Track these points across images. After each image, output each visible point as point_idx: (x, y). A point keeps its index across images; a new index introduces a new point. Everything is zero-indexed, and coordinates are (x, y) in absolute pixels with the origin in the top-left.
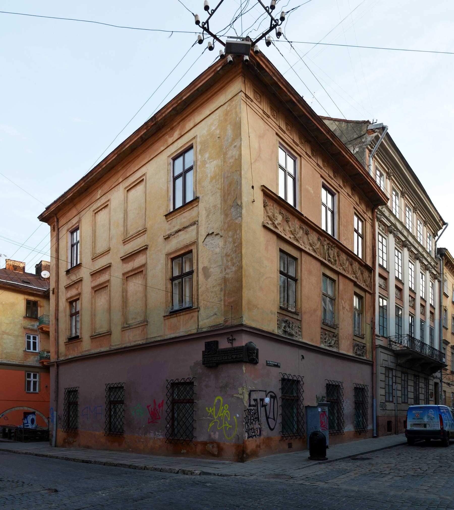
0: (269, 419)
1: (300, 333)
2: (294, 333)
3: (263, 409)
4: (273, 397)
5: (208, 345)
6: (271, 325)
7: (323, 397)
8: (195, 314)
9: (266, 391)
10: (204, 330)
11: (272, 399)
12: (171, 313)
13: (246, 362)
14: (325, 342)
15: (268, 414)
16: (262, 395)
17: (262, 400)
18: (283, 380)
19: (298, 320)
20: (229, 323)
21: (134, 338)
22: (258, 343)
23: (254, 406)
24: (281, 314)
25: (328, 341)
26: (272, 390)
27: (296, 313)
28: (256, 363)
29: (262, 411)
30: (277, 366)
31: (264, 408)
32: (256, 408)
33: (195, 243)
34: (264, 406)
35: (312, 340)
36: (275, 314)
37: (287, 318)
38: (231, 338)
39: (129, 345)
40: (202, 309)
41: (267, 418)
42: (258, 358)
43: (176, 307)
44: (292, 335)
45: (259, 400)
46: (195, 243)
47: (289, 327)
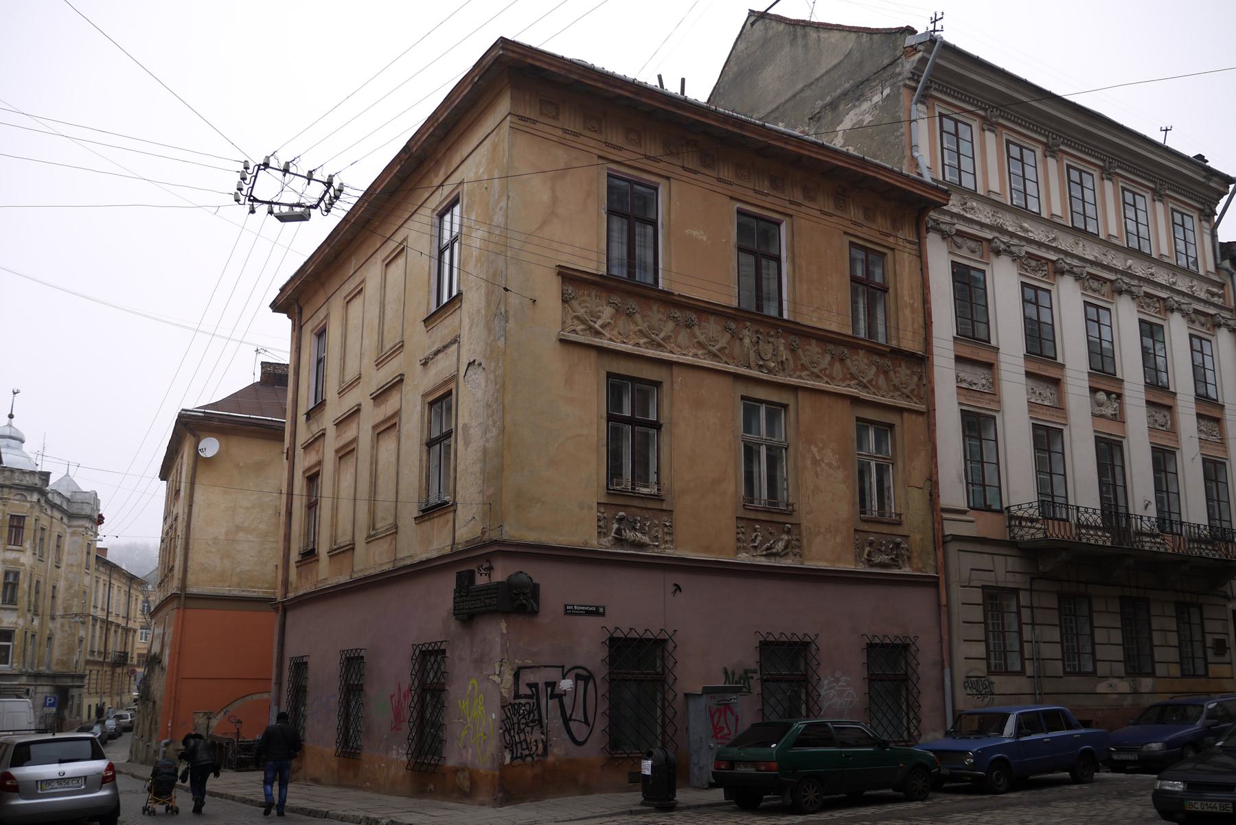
0: (571, 723)
1: (668, 538)
2: (646, 539)
4: (584, 677)
5: (460, 576)
6: (582, 532)
7: (746, 672)
8: (451, 516)
9: (563, 667)
10: (460, 548)
11: (581, 684)
12: (423, 511)
13: (506, 613)
14: (755, 547)
15: (568, 713)
16: (553, 675)
17: (552, 684)
18: (612, 639)
20: (486, 537)
21: (372, 559)
22: (538, 572)
23: (526, 696)
25: (762, 543)
26: (580, 663)
27: (657, 498)
28: (535, 613)
29: (550, 709)
30: (596, 612)
33: (454, 378)
34: (560, 697)
35: (707, 549)
36: (591, 508)
37: (621, 513)
38: (487, 565)
39: (373, 572)
40: (459, 506)
41: (566, 720)
42: (537, 600)
43: (434, 500)
44: (641, 545)
46: (454, 378)
47: (634, 529)
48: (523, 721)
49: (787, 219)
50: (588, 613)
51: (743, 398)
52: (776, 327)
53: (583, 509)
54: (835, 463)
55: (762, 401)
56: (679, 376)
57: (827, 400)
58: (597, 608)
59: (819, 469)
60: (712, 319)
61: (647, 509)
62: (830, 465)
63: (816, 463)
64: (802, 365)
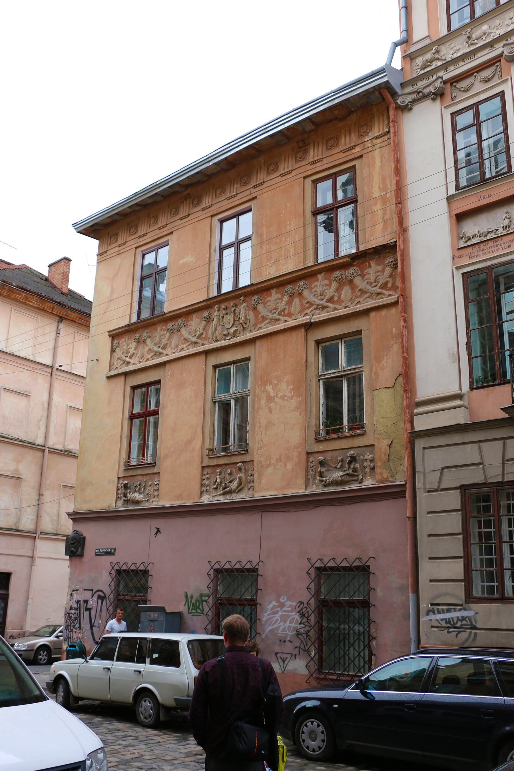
0: (94, 628)
1: (156, 493)
3: (87, 613)
9: (92, 590)
11: (100, 601)
15: (93, 621)
18: (119, 572)
19: (155, 474)
24: (127, 477)
31: (88, 612)
32: (78, 612)
41: (92, 626)
44: (138, 502)
45: (82, 603)
47: (136, 491)
48: (72, 624)
49: (255, 201)
50: (107, 554)
51: (215, 367)
52: (239, 296)
53: (110, 484)
54: (289, 394)
55: (229, 363)
56: (169, 369)
57: (281, 338)
58: (111, 549)
59: (272, 405)
60: (194, 316)
61: (146, 475)
62: (282, 398)
63: (270, 399)
64: (263, 317)
